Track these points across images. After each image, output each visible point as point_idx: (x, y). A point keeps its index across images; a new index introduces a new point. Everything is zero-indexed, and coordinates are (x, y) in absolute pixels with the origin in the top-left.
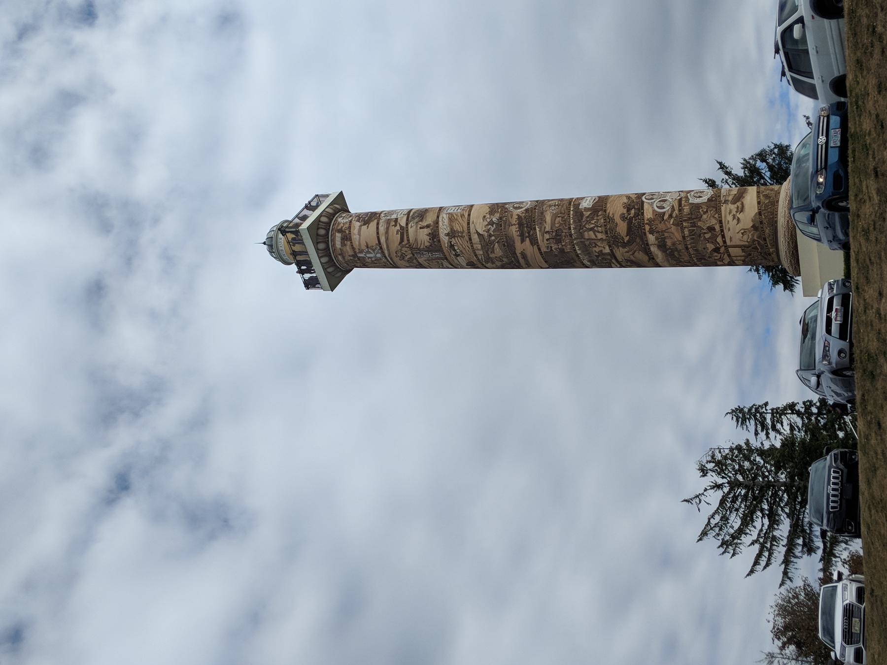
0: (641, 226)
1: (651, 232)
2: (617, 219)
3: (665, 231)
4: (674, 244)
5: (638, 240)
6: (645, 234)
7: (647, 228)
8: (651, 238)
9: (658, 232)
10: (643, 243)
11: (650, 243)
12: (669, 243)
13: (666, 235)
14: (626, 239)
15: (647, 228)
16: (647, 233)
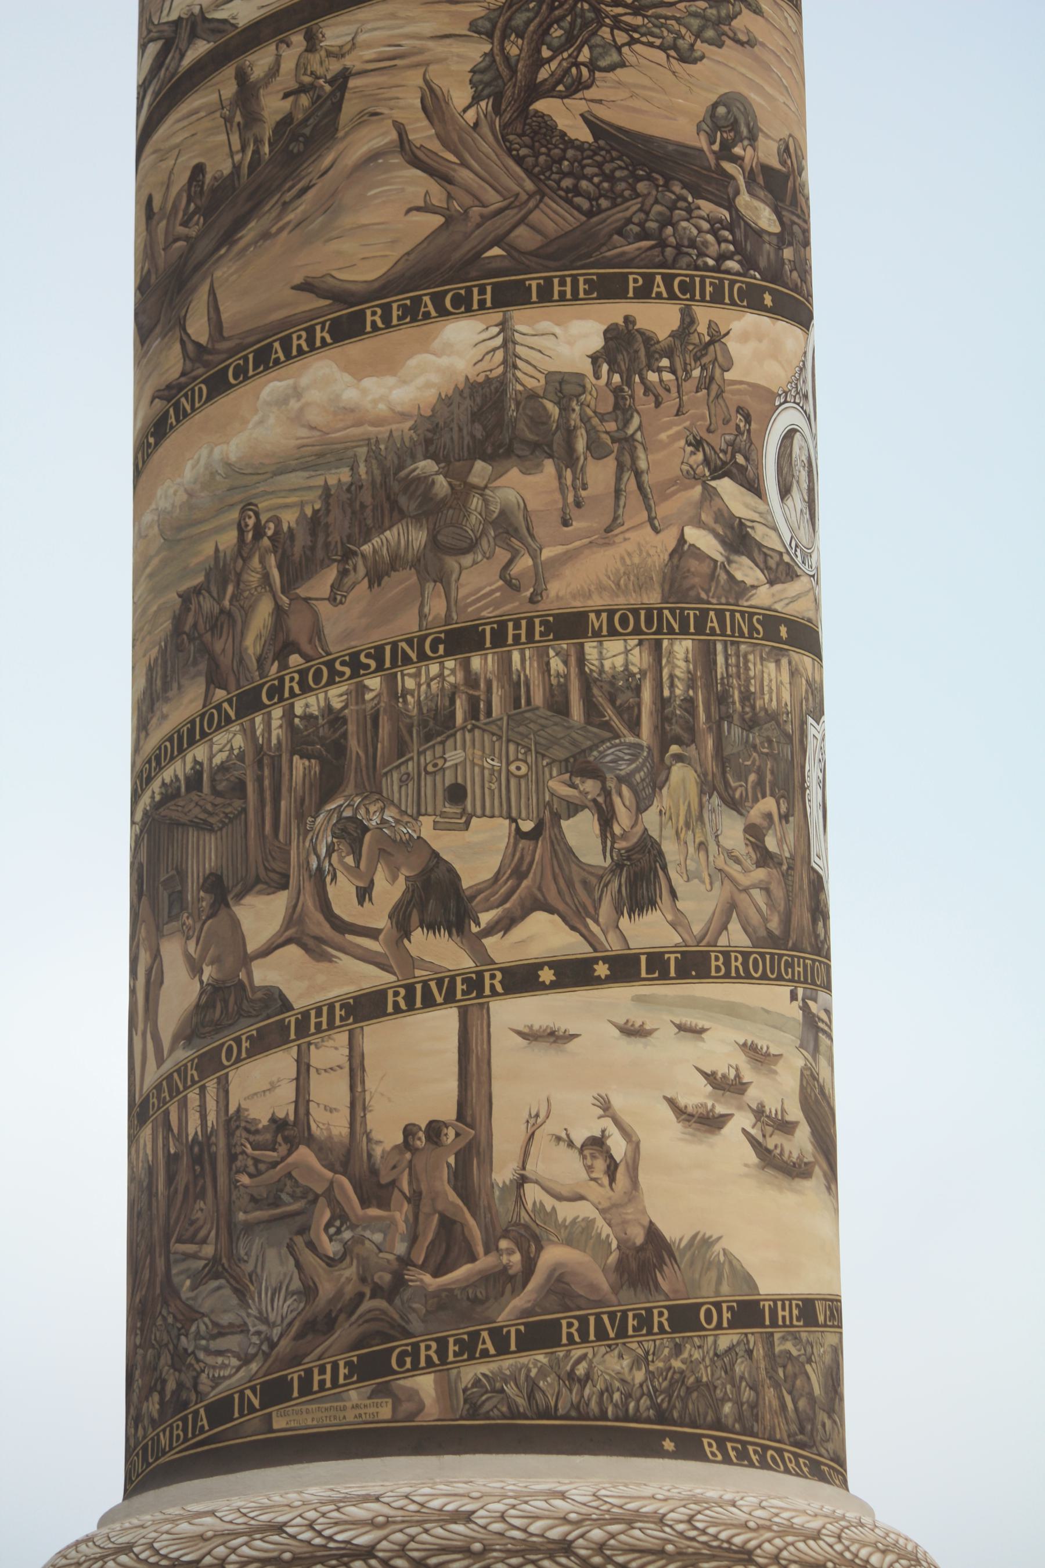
0: (668, 265)
1: (622, 345)
2: (721, 72)
3: (627, 465)
4: (510, 528)
5: (554, 218)
6: (609, 289)
7: (658, 318)
8: (567, 338)
9: (623, 409)
10: (521, 260)
11: (528, 322)
12: (525, 487)
13: (600, 474)
14: (566, 116)
15: (658, 318)
16: (615, 311)
